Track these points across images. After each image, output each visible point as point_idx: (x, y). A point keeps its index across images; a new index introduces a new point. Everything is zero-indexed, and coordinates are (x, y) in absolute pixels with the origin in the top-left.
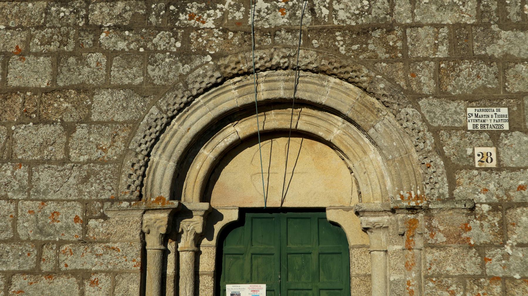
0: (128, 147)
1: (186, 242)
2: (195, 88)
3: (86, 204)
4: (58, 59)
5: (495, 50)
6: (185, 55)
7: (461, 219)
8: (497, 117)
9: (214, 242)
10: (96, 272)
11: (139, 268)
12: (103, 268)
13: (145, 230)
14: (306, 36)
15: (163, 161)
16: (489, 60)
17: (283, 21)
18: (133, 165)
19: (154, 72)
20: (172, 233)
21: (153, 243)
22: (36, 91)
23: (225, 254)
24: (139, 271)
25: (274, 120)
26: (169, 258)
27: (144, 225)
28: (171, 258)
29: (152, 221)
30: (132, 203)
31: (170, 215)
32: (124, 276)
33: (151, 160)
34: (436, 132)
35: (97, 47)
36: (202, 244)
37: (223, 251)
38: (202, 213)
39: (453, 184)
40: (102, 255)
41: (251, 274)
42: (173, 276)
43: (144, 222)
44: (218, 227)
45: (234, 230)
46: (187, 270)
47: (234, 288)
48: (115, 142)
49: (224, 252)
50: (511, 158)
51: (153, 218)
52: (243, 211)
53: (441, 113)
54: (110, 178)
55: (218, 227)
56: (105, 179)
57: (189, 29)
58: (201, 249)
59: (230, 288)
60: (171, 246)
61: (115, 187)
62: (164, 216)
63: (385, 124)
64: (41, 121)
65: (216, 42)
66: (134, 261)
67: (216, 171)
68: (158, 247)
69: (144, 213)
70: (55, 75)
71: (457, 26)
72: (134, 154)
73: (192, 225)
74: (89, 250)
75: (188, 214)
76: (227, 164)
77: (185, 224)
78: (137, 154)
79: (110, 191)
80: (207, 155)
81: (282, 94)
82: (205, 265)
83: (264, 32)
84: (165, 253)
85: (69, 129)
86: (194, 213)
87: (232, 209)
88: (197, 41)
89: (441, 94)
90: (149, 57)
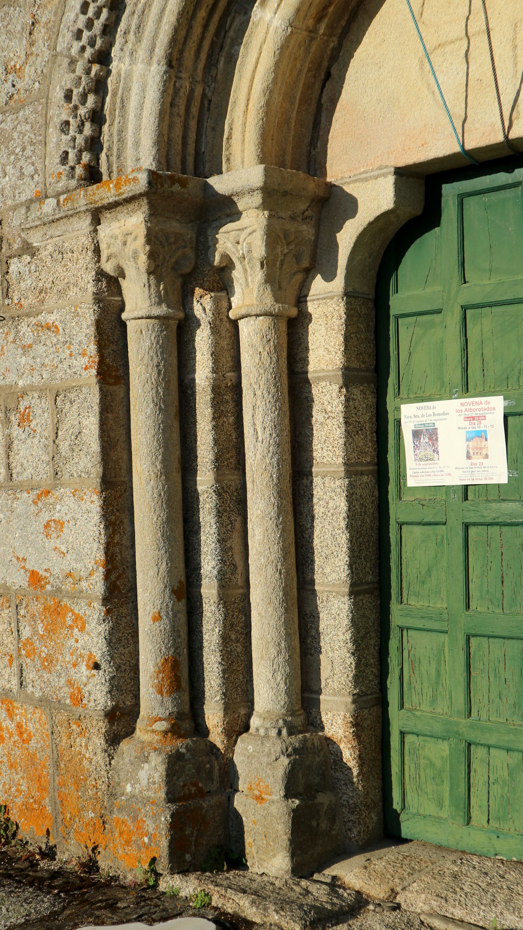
0: (55, 49)
1: (249, 291)
9: (338, 284)
10: (24, 393)
11: (94, 372)
12: (36, 379)
13: (108, 267)
15: (139, 68)
18: (68, 97)
21: (138, 299)
23: (397, 318)
24: (94, 380)
26: (198, 339)
27: (104, 258)
28: (203, 340)
29: (119, 242)
30: (62, 198)
31: (154, 214)
32: (72, 396)
33: (114, 71)
36: (311, 293)
37: (389, 307)
38: (257, 199)
40: (30, 346)
41: (466, 370)
42: (209, 389)
43: (103, 246)
44: (347, 237)
45: (418, 241)
46: (254, 370)
47: (419, 413)
48: (32, 44)
49: (393, 312)
51: (117, 232)
54: (32, 144)
55: (347, 237)
56: (24, 149)
58: (311, 307)
59: (410, 415)
60: (203, 306)
61: (39, 166)
66: (84, 355)
67: (334, 71)
68: (157, 311)
69: (96, 221)
72: (66, 62)
73: (243, 241)
74: (11, 338)
76: (358, 42)
78: (73, 62)
79: (32, 177)
82: (321, 351)
86: (241, 205)
87: (376, 177)
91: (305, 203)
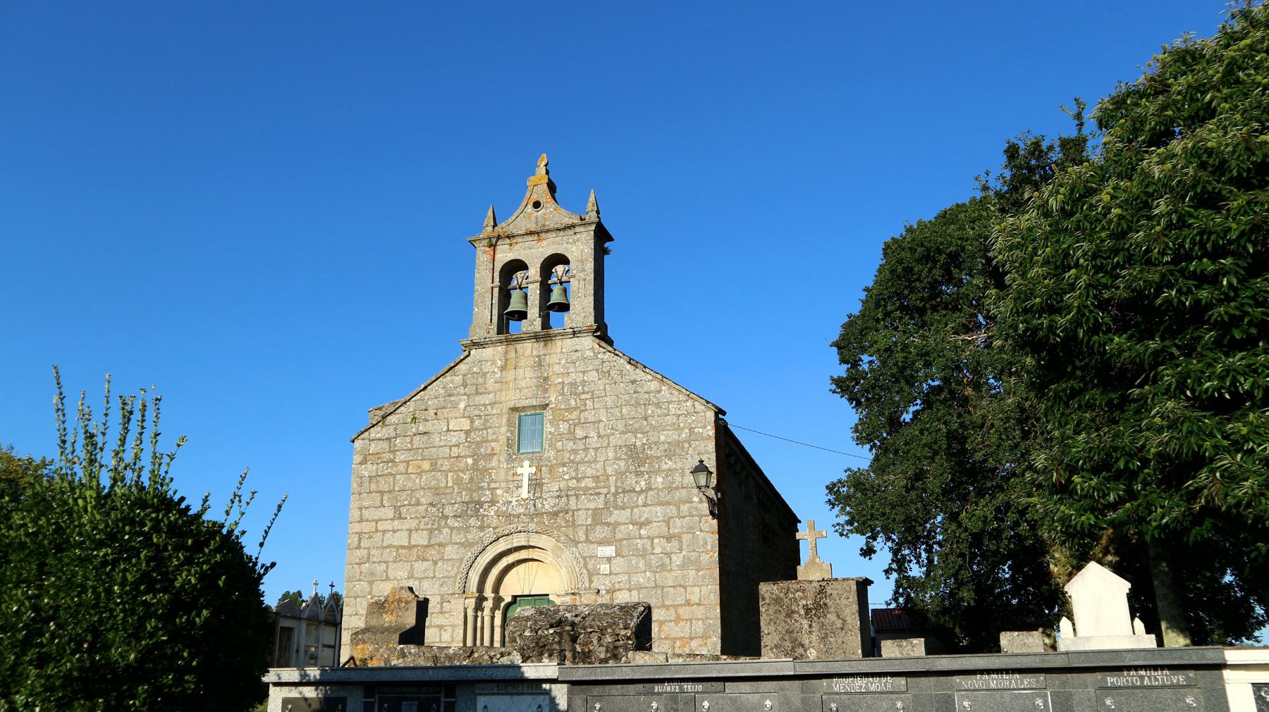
1: (487, 612)
2: (486, 543)
3: (442, 596)
4: (431, 531)
5: (611, 519)
6: (482, 528)
7: (594, 597)
8: (609, 551)
14: (532, 517)
16: (608, 524)
17: (522, 510)
19: (470, 536)
20: (479, 607)
21: (470, 613)
22: (423, 546)
25: (523, 555)
34: (584, 558)
35: (447, 525)
39: (591, 582)
44: (502, 605)
50: (616, 569)
52: (515, 597)
53: (586, 549)
55: (502, 605)
57: (484, 516)
62: (473, 600)
63: (567, 554)
64: (425, 560)
65: (495, 522)
70: (430, 539)
71: (596, 509)
73: (488, 605)
75: (486, 599)
77: (485, 604)
80: (495, 572)
81: (523, 543)
83: (514, 516)
84: (476, 617)
85: (435, 563)
88: (487, 521)
89: (588, 541)
90: (467, 529)
91: (498, 600)
